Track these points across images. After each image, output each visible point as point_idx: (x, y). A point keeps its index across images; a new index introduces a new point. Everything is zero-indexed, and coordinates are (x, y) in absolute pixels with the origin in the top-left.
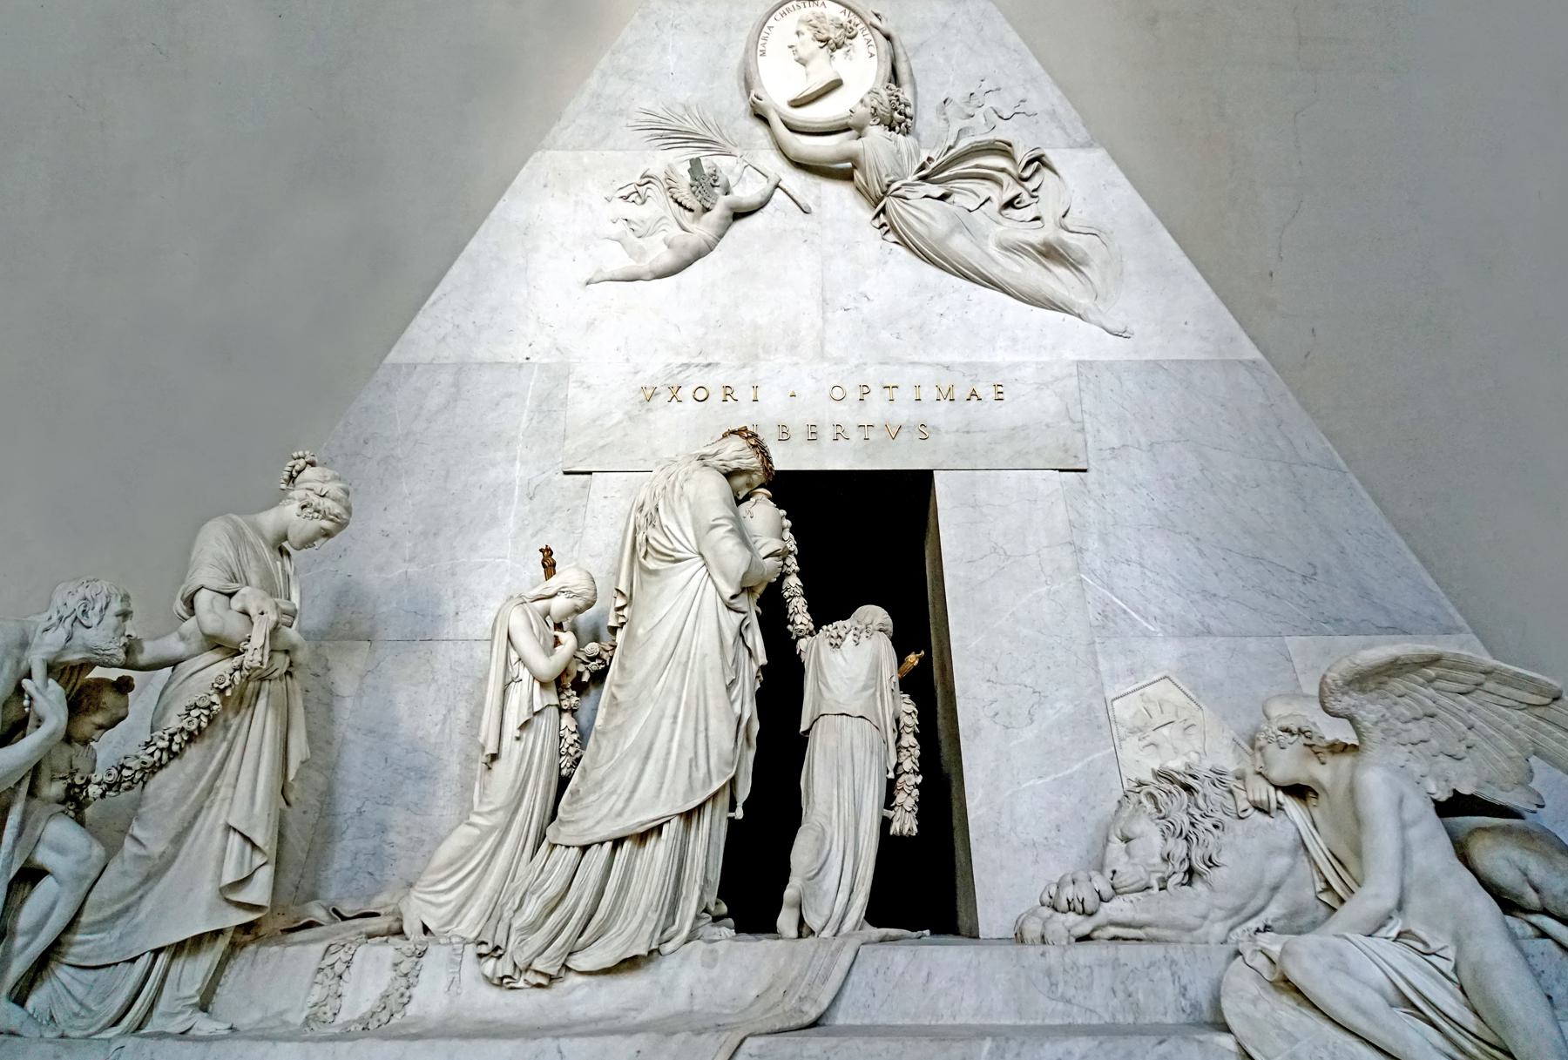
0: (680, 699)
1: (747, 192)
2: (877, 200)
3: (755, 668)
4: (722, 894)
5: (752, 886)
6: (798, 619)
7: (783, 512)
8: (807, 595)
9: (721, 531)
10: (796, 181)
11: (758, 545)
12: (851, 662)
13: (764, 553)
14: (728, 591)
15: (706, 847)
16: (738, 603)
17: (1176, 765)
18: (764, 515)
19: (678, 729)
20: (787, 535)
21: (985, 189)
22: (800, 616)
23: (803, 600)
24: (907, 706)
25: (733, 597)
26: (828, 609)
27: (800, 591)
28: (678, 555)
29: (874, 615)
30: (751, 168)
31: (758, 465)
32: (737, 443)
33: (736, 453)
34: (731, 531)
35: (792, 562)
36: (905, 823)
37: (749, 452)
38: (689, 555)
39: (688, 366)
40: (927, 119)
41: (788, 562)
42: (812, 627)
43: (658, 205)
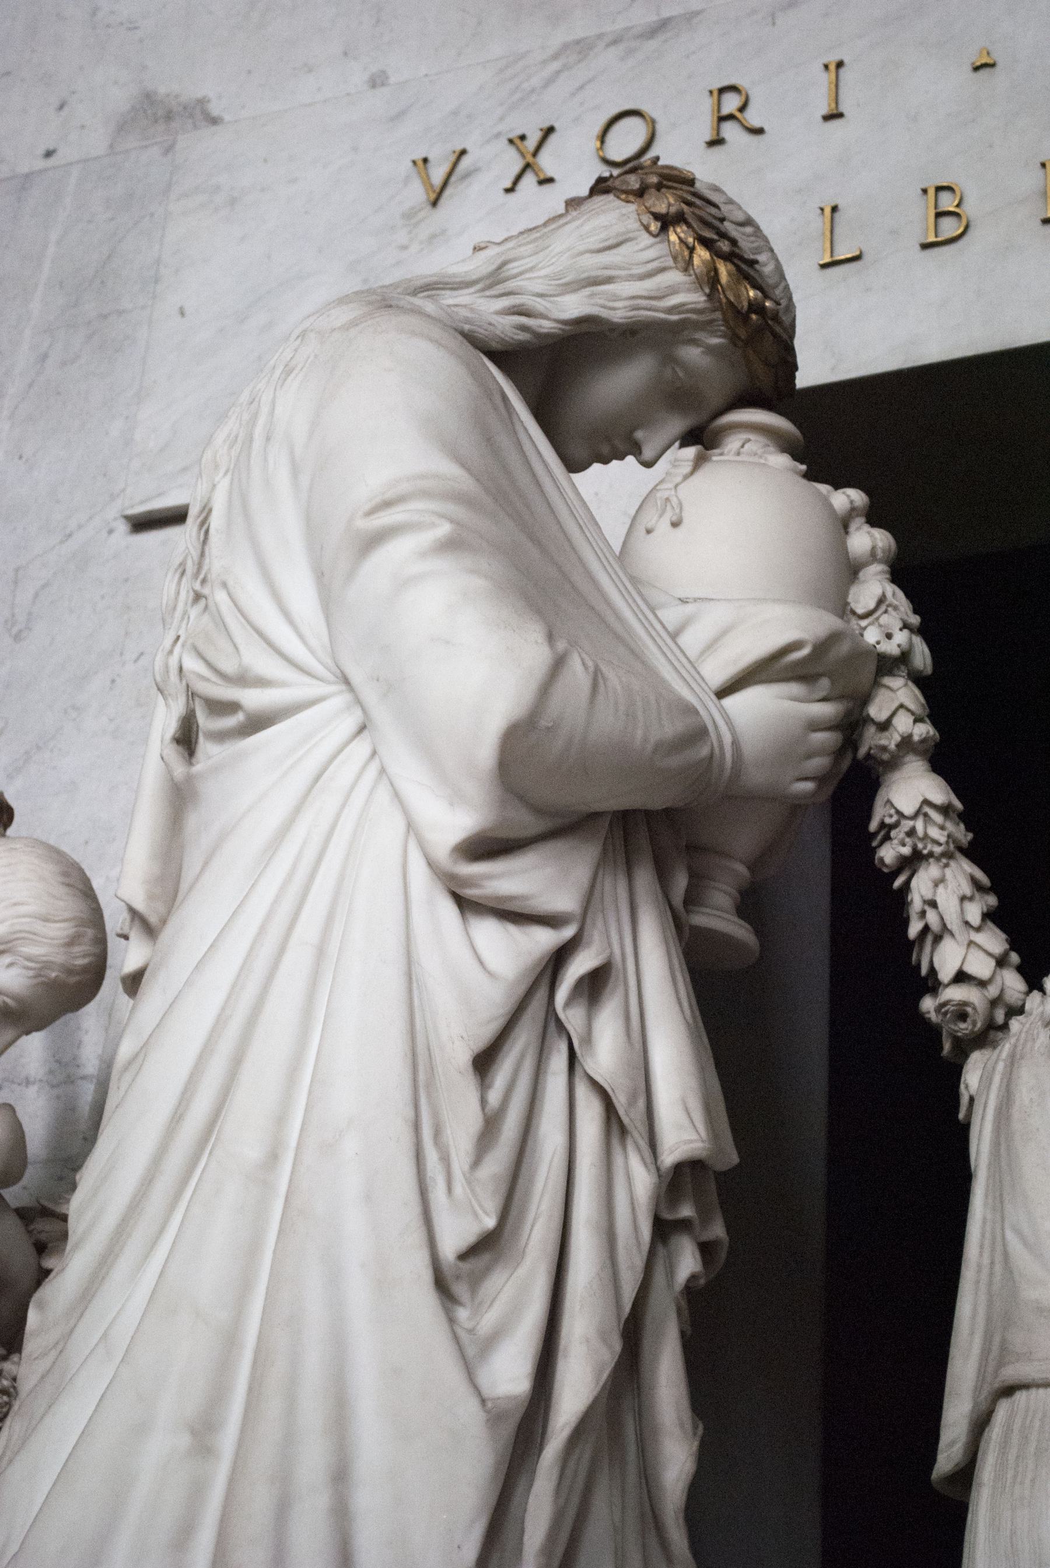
0: (231, 1340)
3: (639, 1181)
6: (948, 958)
7: (847, 498)
8: (992, 841)
9: (398, 552)
11: (692, 641)
13: (718, 670)
14: (453, 821)
16: (510, 879)
20: (873, 587)
23: (961, 874)
25: (484, 848)
27: (938, 832)
28: (253, 699)
31: (696, 298)
32: (617, 216)
34: (451, 545)
35: (899, 709)
37: (646, 249)
38: (300, 689)
39: (582, 48)
41: (877, 711)
42: (1013, 983)
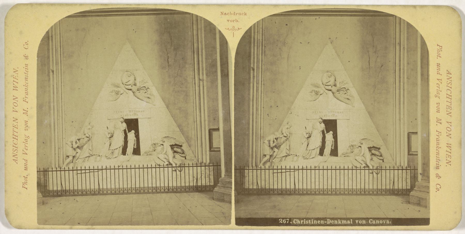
1: (321, 93)
2: (333, 93)
4: (320, 153)
5: (321, 153)
10: (327, 91)
12: (329, 136)
15: (318, 151)
17: (352, 144)
18: (323, 125)
19: (316, 142)
21: (343, 92)
22: (325, 132)
24: (333, 140)
26: (328, 132)
29: (331, 132)
30: (321, 91)
33: (321, 120)
36: (333, 148)
40: (338, 85)
43: (314, 93)
